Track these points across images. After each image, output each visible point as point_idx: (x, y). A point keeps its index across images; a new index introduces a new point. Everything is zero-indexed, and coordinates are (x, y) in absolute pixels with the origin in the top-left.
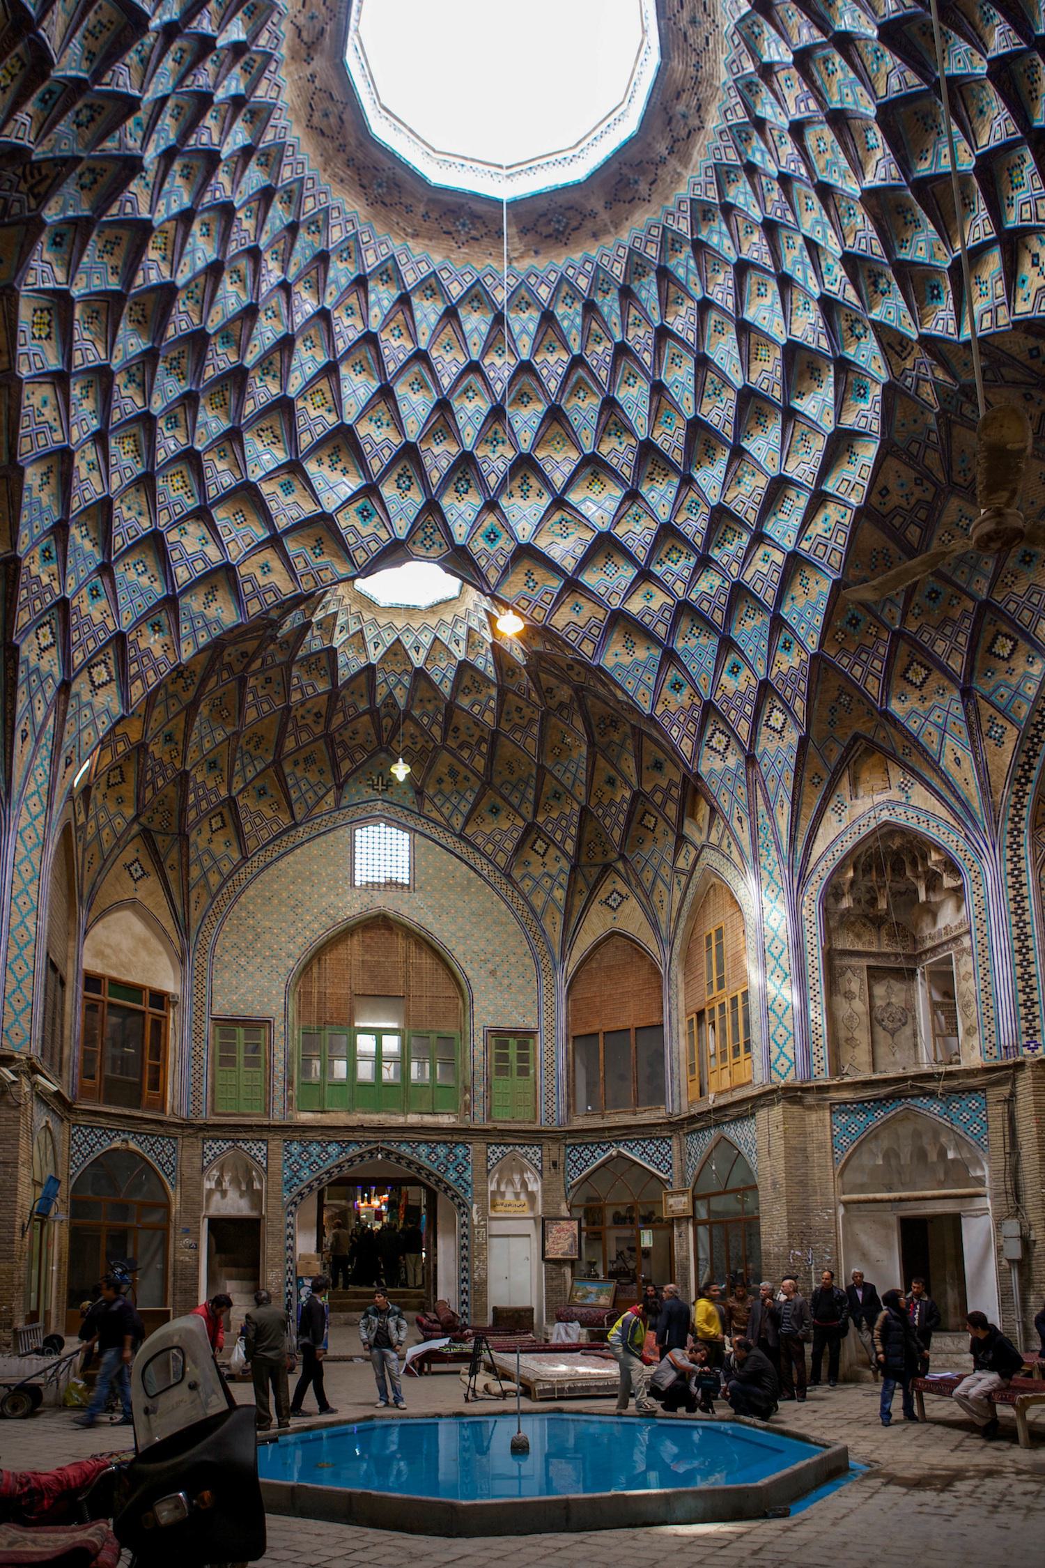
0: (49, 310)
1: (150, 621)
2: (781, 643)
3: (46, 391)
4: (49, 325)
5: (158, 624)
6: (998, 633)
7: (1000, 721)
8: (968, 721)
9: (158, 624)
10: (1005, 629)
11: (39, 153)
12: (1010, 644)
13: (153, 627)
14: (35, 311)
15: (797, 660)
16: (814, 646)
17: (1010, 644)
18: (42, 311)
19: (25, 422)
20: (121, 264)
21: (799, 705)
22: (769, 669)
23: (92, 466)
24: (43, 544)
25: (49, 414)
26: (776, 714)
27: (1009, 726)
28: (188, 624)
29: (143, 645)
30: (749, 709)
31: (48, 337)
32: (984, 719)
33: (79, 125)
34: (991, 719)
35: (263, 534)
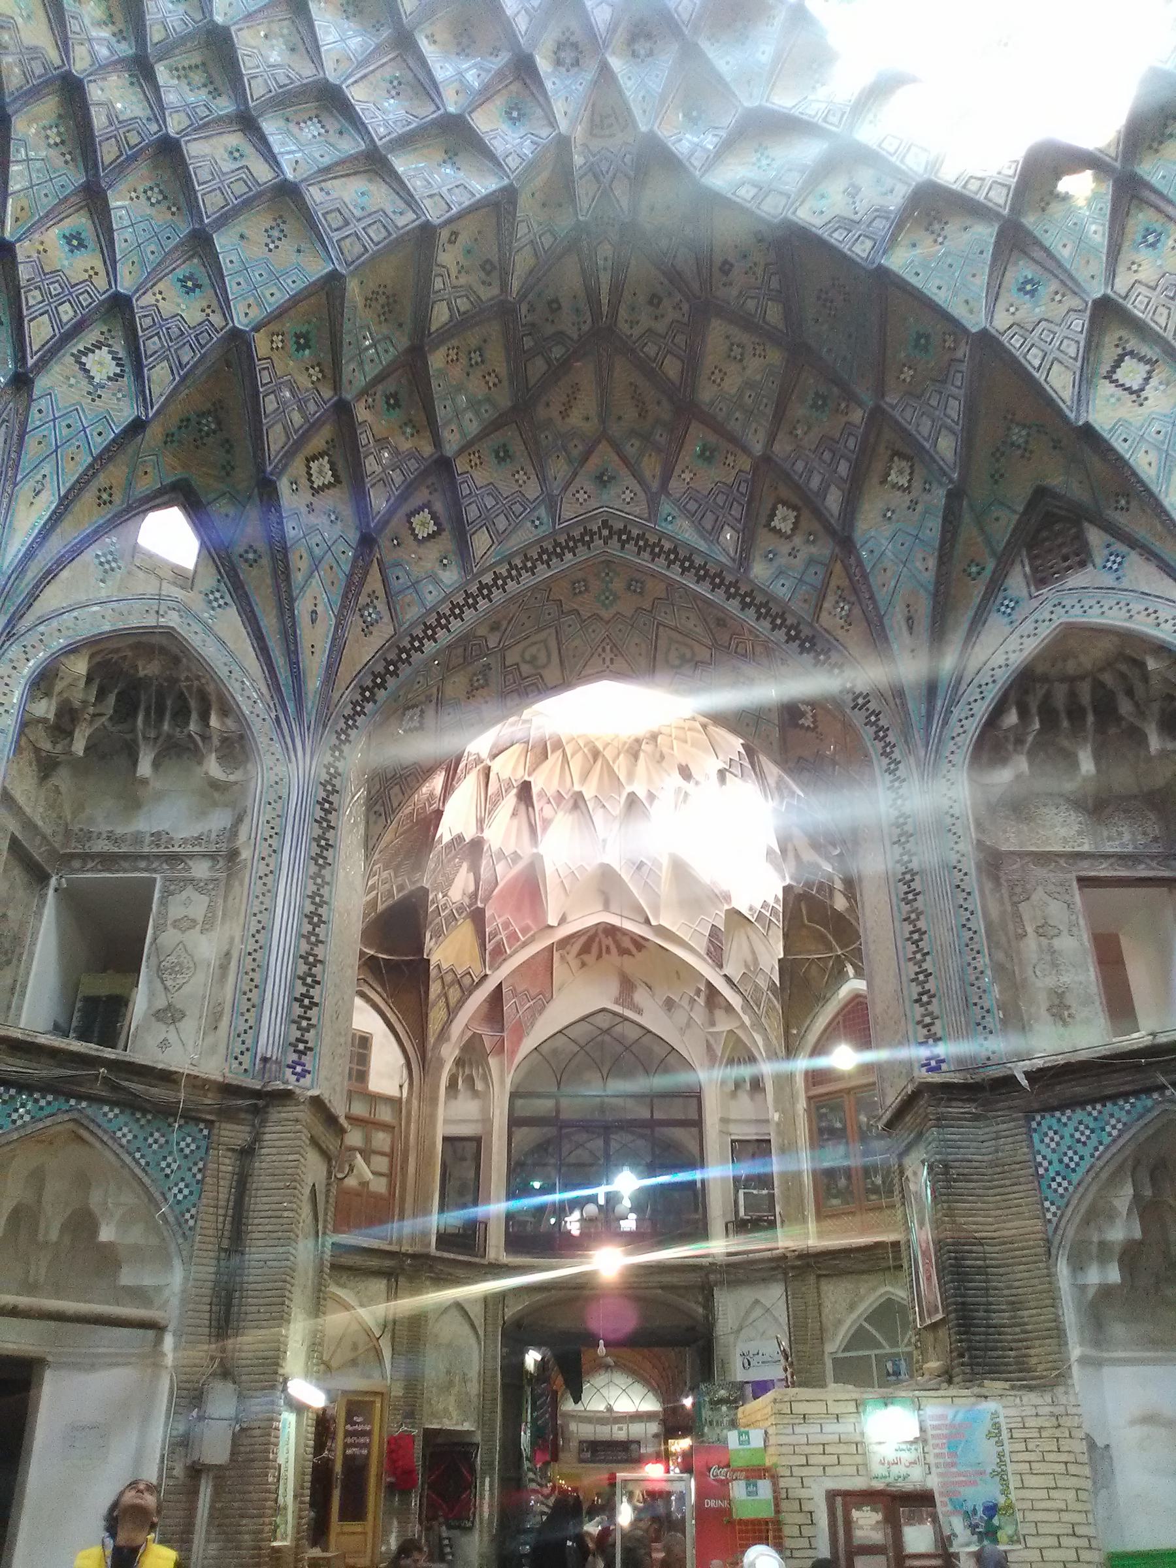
2: (180, 273)
6: (427, 505)
7: (381, 605)
8: (350, 577)
10: (438, 506)
12: (432, 528)
15: (200, 317)
16: (245, 321)
17: (432, 528)
21: (160, 378)
22: (142, 288)
26: (103, 354)
27: (386, 618)
30: (67, 312)
32: (367, 589)
34: (372, 595)
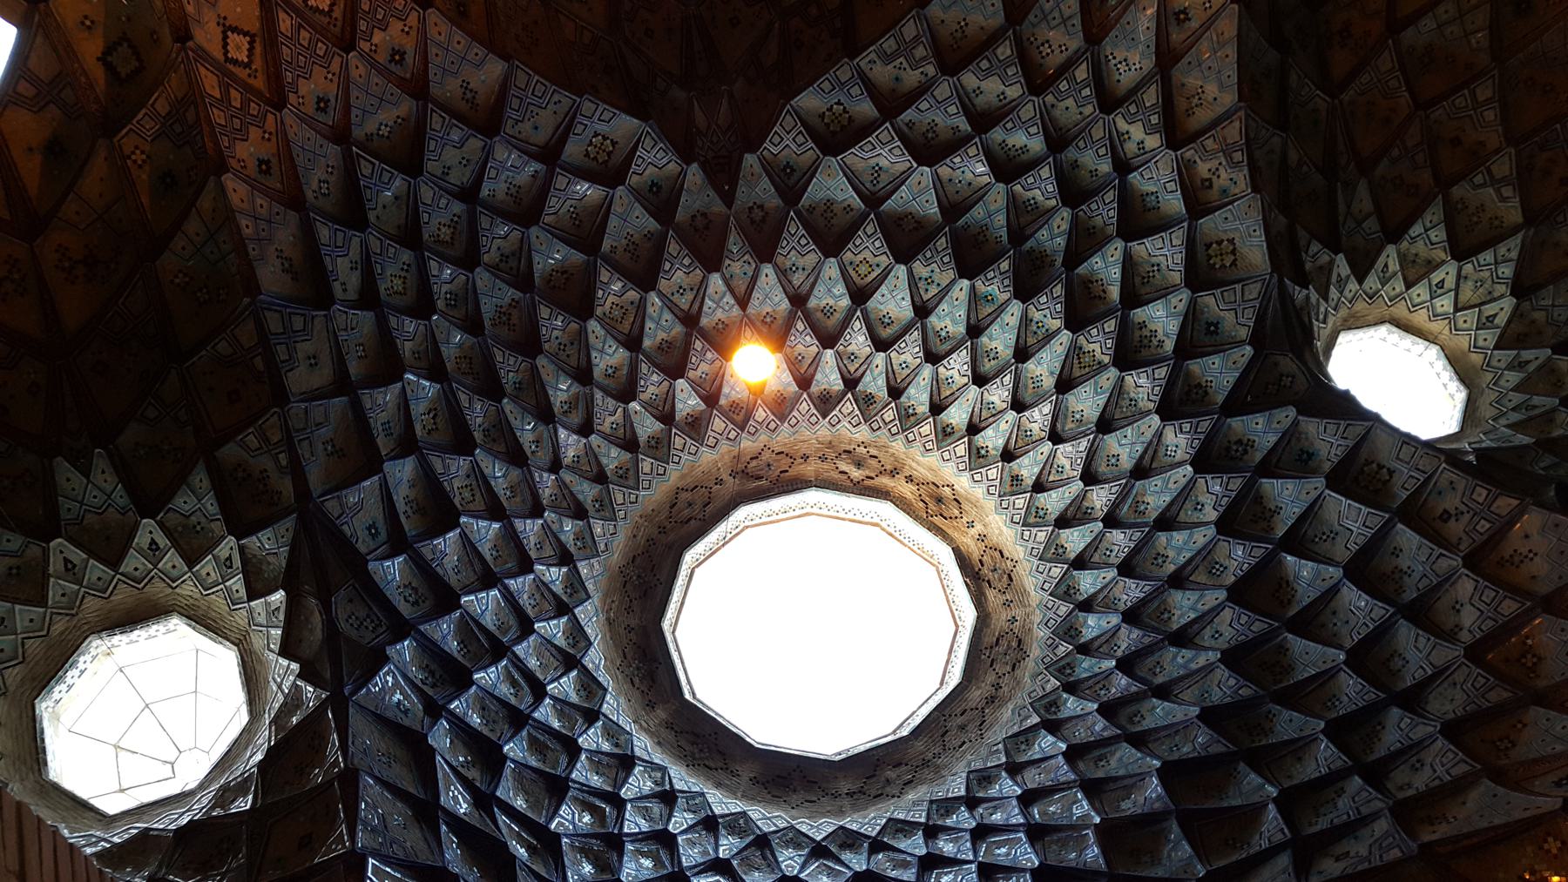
0: (605, 162)
1: (274, 161)
3: (541, 137)
4: (595, 159)
5: (267, 172)
9: (267, 172)
11: (750, 159)
13: (268, 162)
14: (614, 143)
18: (609, 154)
19: (540, 89)
20: (617, 257)
23: (447, 170)
24: (409, 59)
25: (526, 127)
28: (264, 212)
29: (254, 133)
31: (587, 155)
33: (751, 209)
35: (354, 369)
